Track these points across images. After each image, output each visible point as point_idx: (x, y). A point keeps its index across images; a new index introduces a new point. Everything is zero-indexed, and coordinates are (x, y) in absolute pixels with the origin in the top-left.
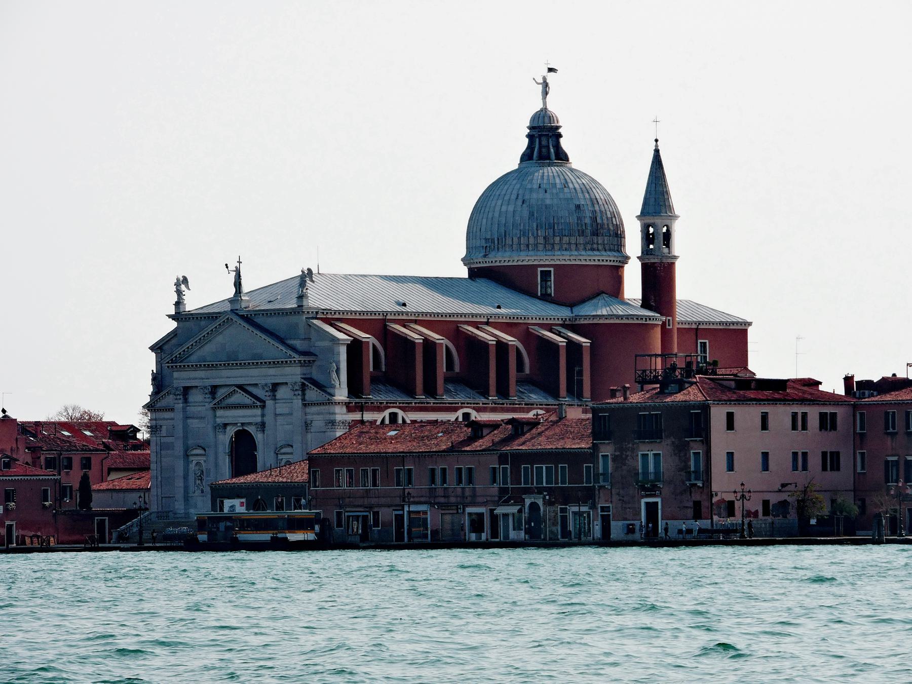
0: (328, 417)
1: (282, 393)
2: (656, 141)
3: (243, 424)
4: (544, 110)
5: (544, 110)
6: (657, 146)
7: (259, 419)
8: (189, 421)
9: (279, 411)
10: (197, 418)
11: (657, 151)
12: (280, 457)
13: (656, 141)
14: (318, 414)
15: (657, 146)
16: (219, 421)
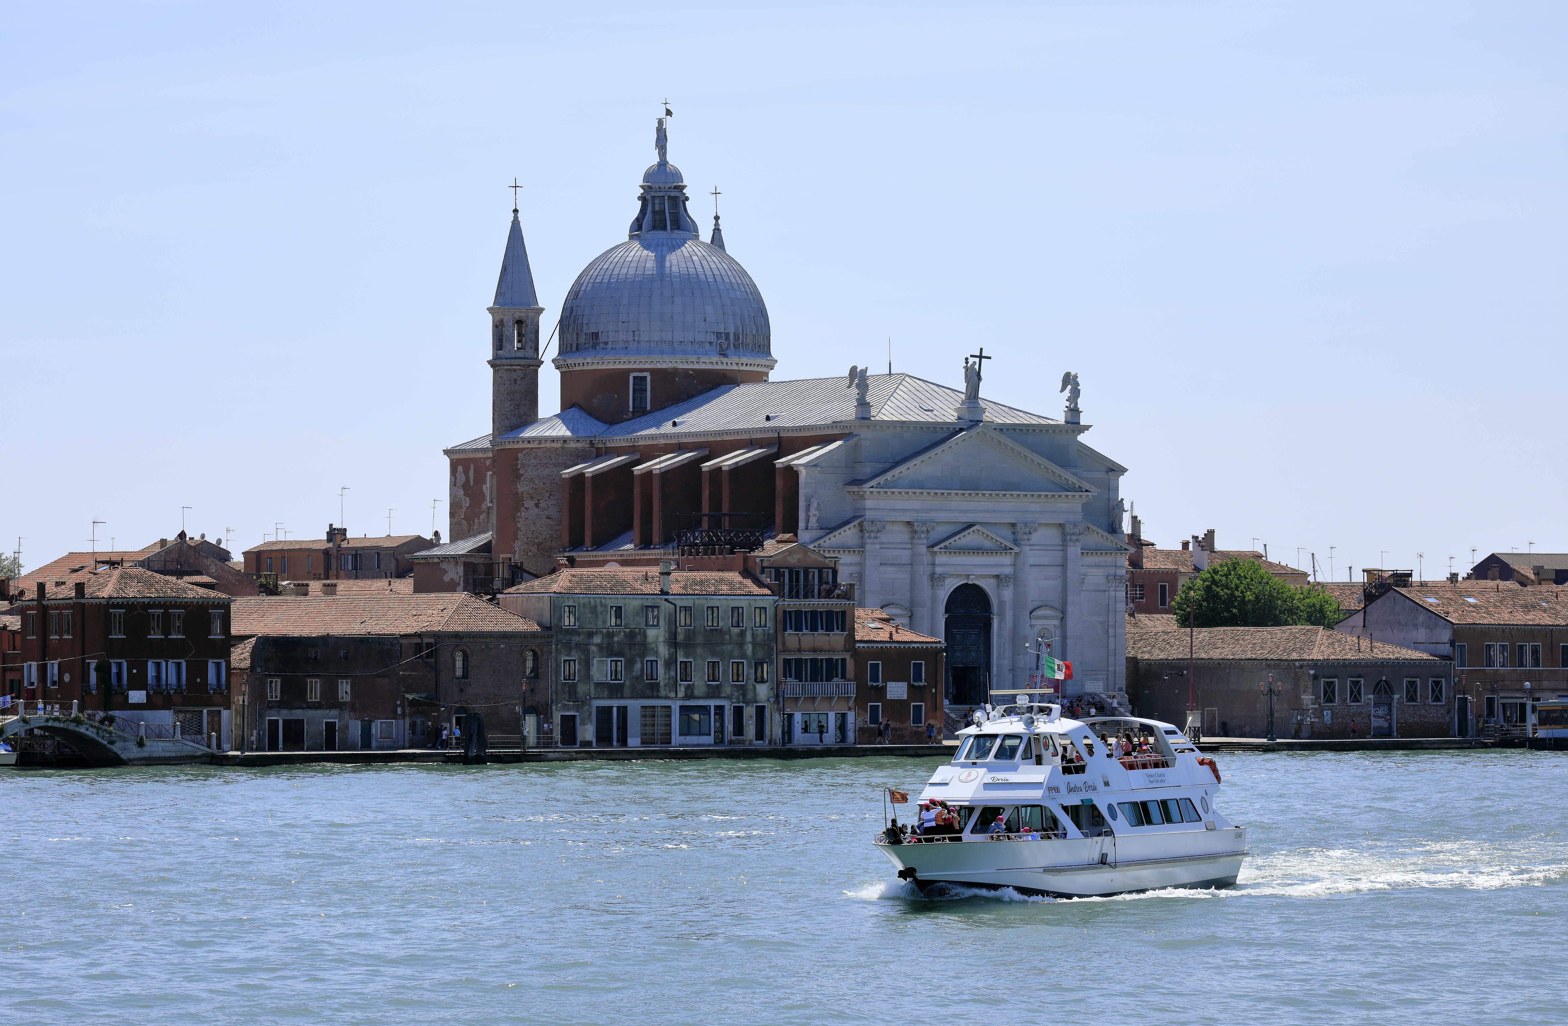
0: (1112, 571)
1: (1035, 538)
2: (717, 218)
3: (979, 577)
4: (663, 163)
5: (663, 163)
6: (717, 224)
7: (1008, 570)
8: (882, 568)
9: (1032, 561)
10: (894, 565)
11: (717, 230)
12: (1034, 622)
13: (717, 218)
14: (1098, 566)
15: (717, 224)
16: (938, 570)
